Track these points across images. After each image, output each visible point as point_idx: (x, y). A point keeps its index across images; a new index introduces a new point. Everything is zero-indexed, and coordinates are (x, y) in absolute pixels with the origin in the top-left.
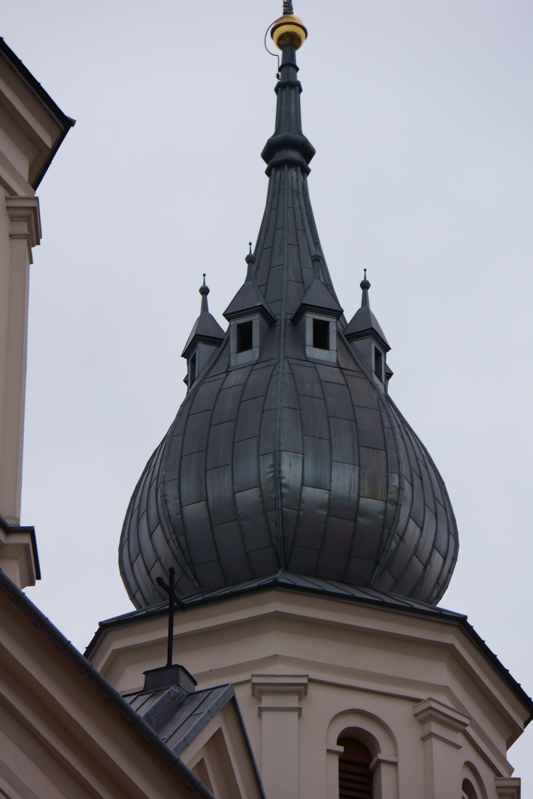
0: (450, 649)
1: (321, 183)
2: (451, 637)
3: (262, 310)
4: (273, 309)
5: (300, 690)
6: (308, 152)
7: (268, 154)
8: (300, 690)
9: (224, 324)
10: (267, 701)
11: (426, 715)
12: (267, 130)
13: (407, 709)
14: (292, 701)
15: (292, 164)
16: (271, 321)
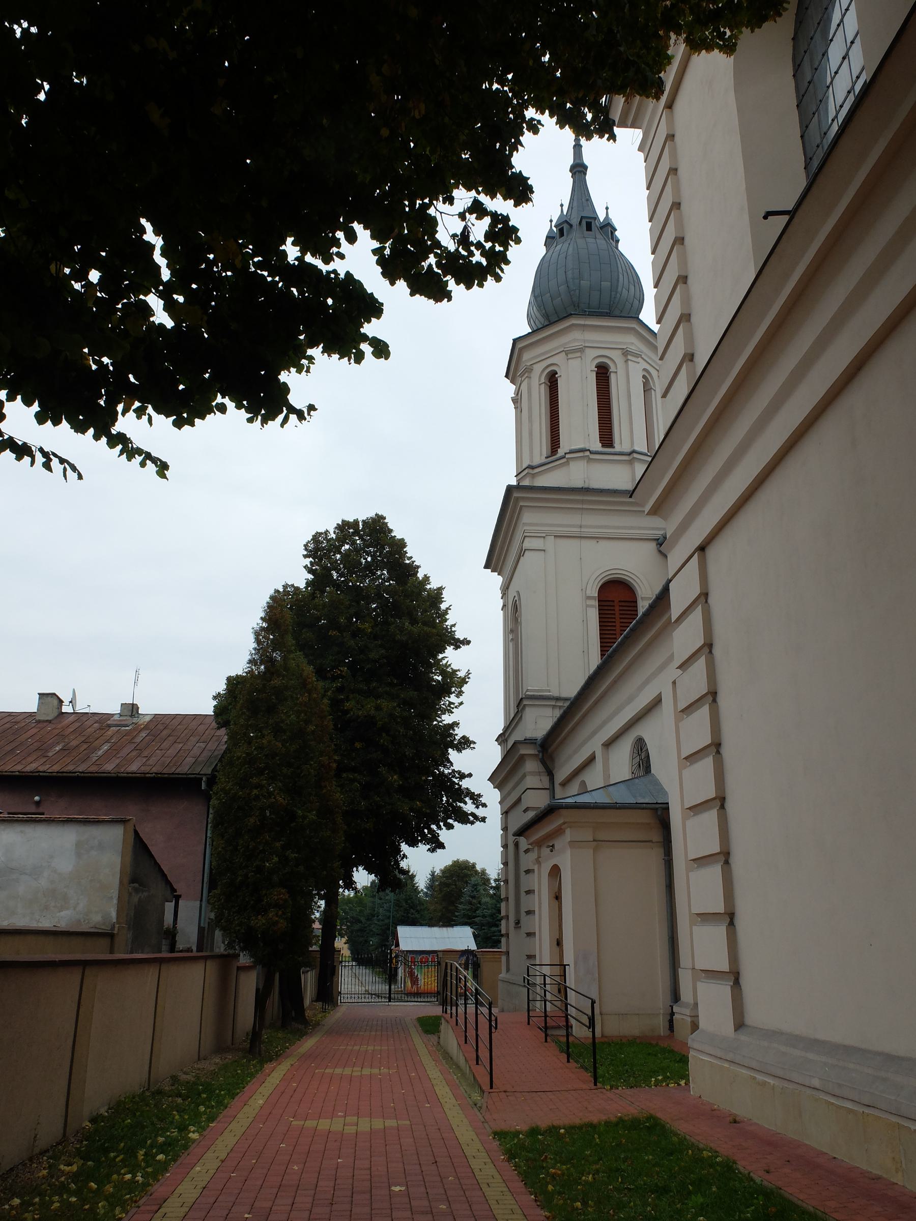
0: (633, 329)
1: (590, 178)
2: (634, 325)
3: (566, 222)
4: (571, 222)
5: (581, 350)
6: (586, 168)
7: (571, 171)
8: (581, 350)
9: (555, 229)
10: (570, 356)
11: (626, 353)
12: (570, 161)
13: (619, 352)
14: (578, 354)
15: (580, 172)
16: (571, 226)
